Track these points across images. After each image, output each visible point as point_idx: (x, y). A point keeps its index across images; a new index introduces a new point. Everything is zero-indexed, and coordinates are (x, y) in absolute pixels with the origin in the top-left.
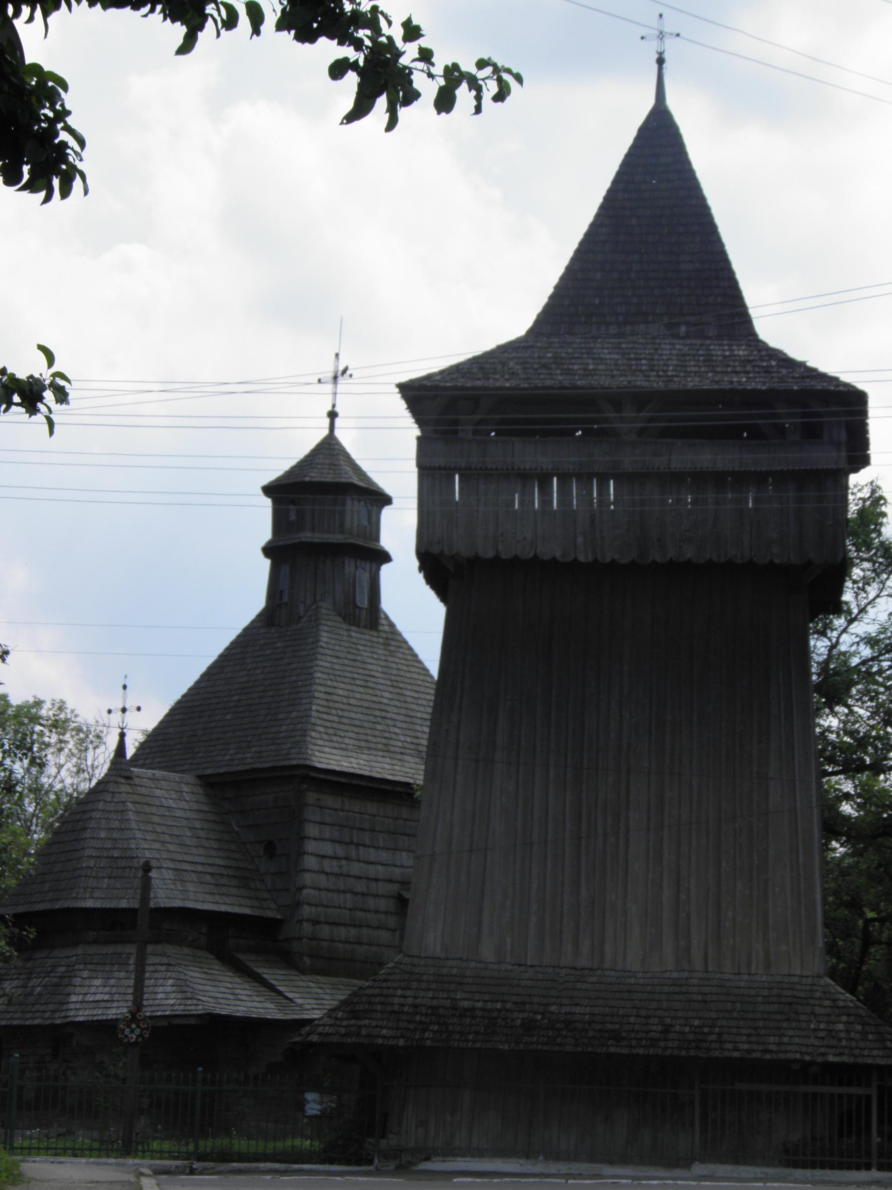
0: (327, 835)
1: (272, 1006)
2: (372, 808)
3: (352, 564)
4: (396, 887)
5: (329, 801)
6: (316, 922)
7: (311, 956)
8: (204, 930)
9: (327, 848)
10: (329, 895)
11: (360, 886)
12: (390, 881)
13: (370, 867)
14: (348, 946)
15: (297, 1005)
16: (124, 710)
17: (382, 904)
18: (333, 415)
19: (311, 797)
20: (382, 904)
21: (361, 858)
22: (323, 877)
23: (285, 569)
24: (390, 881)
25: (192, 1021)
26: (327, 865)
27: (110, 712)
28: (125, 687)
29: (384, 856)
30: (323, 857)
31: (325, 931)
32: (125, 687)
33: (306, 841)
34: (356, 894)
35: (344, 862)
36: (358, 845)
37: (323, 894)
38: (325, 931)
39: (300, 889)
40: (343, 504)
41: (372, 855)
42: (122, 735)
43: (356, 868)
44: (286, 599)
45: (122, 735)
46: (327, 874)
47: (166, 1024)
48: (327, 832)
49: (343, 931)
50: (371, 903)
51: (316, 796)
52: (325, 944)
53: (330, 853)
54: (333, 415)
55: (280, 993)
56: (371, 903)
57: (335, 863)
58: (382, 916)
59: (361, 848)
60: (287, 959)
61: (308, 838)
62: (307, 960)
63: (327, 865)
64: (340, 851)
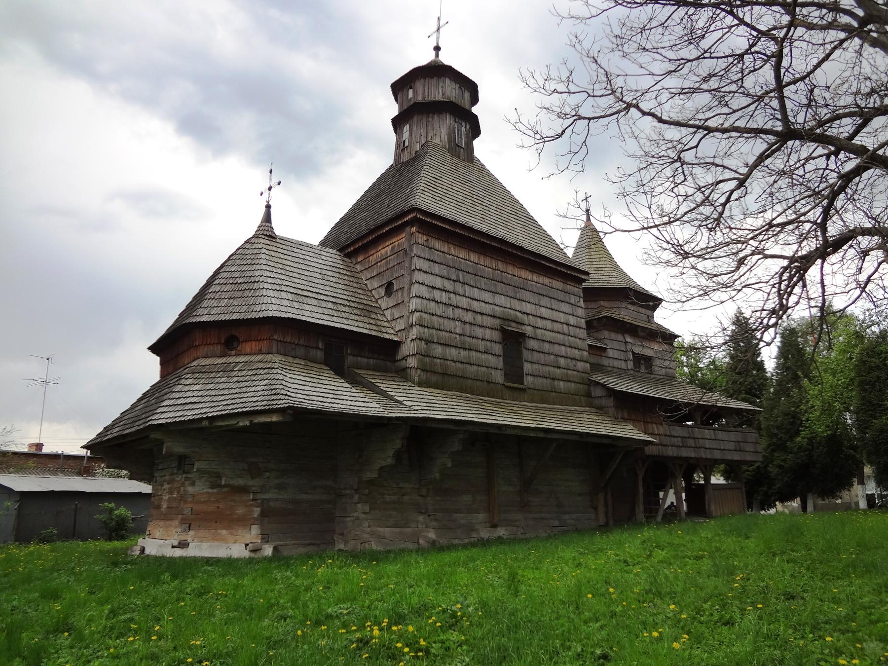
0: (437, 272)
1: (374, 405)
2: (474, 257)
3: (453, 119)
4: (498, 321)
5: (437, 244)
6: (428, 342)
7: (422, 370)
8: (320, 346)
9: (438, 282)
10: (441, 320)
11: (468, 317)
12: (493, 316)
13: (475, 302)
14: (460, 365)
15: (406, 406)
16: (270, 189)
17: (488, 333)
18: (437, 49)
19: (421, 238)
20: (488, 333)
21: (467, 295)
22: (433, 304)
23: (407, 128)
24: (493, 316)
25: (275, 418)
26: (437, 295)
27: (262, 194)
28: (271, 172)
29: (487, 296)
30: (433, 288)
31: (438, 350)
32: (271, 172)
33: (416, 272)
34: (465, 323)
35: (452, 295)
36: (464, 284)
37: (435, 318)
38: (438, 350)
39: (412, 312)
40: (444, 82)
41: (476, 293)
42: (268, 207)
43: (464, 302)
44: (407, 144)
45: (268, 207)
46: (437, 302)
47: (248, 423)
48: (437, 269)
49: (454, 352)
50: (479, 332)
51: (425, 238)
52: (438, 361)
53: (439, 285)
54: (437, 49)
55: (391, 398)
56: (479, 332)
57: (444, 293)
58: (488, 343)
59: (466, 286)
60: (402, 374)
61: (419, 270)
62: (424, 375)
63: (437, 295)
64: (449, 286)
